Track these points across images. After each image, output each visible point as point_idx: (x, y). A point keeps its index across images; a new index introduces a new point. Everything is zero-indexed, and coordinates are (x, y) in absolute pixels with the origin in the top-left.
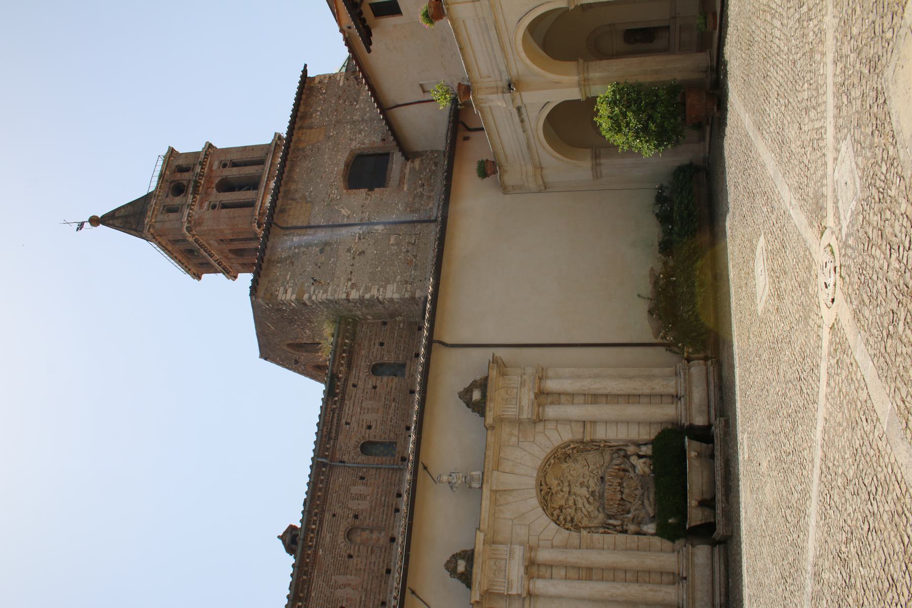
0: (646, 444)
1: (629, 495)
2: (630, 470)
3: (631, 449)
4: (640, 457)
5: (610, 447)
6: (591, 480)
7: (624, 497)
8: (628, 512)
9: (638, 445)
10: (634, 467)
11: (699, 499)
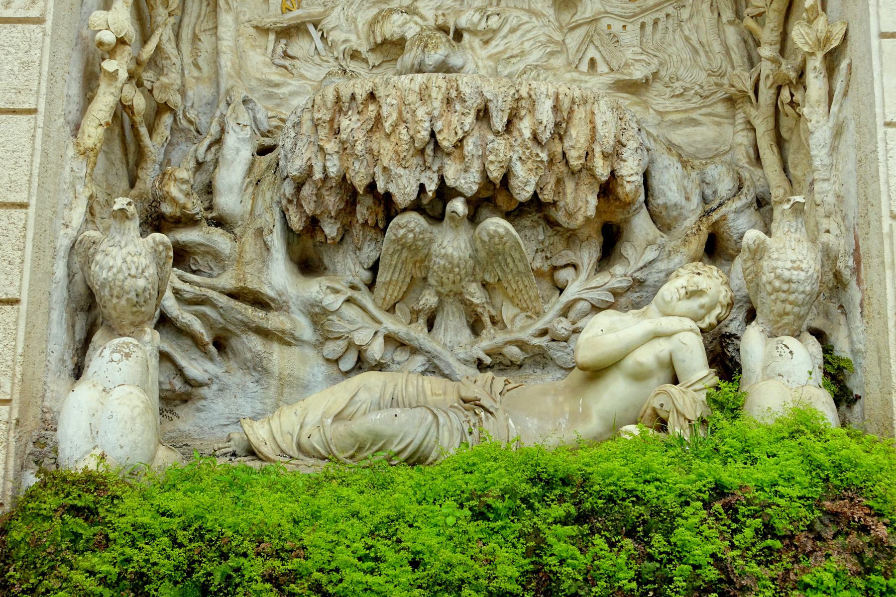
1: (418, 255)
2: (618, 275)
3: (789, 255)
8: (307, 266)
10: (636, 294)
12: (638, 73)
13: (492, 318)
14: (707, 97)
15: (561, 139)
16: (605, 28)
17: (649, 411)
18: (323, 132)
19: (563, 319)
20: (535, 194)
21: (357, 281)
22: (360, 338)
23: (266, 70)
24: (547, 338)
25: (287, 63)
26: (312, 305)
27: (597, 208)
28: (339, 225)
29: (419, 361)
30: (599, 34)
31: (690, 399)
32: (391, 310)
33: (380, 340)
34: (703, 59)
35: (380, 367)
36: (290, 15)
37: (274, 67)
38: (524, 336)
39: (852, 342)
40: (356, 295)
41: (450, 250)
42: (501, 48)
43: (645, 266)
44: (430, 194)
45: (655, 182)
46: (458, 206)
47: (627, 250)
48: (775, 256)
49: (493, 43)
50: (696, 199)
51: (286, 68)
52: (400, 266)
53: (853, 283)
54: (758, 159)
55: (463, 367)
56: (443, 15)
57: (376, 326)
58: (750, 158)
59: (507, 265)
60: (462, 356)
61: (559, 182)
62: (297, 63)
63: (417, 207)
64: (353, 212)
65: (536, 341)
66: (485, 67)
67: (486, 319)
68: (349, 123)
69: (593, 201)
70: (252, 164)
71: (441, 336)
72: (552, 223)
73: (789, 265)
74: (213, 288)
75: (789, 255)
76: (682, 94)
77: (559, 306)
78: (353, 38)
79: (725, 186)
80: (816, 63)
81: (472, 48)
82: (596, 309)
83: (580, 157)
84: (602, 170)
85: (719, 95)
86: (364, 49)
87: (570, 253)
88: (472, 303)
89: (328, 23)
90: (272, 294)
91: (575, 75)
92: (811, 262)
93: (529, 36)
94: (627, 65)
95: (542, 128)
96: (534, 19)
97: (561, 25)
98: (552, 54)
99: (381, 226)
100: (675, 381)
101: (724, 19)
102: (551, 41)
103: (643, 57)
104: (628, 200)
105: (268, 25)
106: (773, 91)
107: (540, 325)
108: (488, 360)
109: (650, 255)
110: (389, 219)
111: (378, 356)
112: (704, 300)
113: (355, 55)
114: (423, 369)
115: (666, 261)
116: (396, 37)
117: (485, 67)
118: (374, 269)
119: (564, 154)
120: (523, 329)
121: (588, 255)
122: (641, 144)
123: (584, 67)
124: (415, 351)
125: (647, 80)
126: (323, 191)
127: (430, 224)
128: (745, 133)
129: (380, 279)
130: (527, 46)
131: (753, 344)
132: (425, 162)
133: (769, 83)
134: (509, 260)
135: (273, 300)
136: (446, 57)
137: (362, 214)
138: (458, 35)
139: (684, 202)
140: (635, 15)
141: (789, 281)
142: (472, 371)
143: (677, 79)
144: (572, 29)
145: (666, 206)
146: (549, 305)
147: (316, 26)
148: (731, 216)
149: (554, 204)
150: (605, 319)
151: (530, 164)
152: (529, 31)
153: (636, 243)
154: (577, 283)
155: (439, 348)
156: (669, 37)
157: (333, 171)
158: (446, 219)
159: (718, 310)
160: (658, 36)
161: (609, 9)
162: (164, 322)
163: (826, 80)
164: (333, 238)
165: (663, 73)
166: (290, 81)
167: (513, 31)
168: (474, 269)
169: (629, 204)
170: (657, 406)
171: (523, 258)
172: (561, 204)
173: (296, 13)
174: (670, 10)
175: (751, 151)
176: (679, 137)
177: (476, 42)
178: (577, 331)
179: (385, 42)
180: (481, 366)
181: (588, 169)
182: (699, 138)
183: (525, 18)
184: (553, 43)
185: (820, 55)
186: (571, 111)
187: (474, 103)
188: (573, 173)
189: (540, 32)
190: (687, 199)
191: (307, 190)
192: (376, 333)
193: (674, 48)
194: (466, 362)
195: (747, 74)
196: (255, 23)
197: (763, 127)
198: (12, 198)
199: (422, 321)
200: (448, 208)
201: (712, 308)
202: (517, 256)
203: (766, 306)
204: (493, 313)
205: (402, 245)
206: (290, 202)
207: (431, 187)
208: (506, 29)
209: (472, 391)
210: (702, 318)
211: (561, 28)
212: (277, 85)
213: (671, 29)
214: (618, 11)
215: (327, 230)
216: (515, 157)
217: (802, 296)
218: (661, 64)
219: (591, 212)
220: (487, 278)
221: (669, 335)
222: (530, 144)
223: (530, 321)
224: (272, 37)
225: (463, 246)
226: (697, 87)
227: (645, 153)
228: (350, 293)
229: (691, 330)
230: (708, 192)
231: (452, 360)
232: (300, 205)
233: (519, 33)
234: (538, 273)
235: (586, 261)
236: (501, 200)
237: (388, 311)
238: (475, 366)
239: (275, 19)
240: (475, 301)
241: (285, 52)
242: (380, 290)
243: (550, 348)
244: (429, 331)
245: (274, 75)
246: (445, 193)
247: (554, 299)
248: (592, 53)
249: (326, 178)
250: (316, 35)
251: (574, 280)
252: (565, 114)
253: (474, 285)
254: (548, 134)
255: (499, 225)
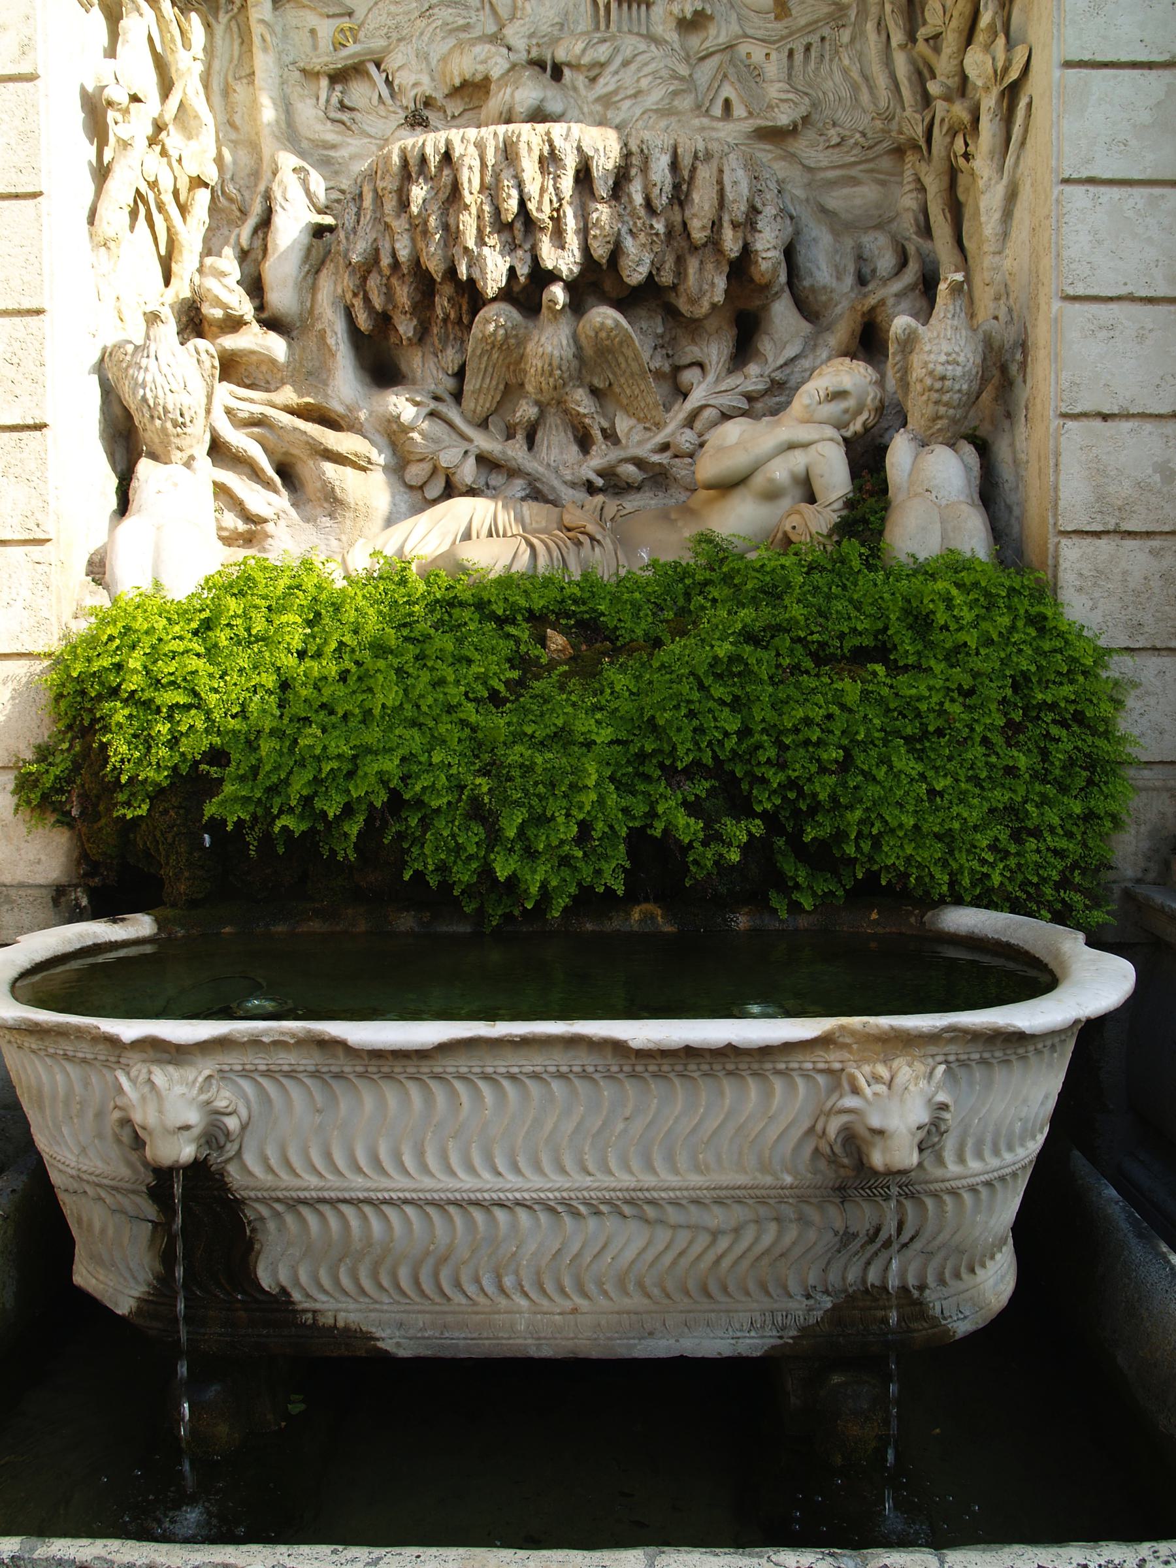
0: (989, 492)
2: (753, 377)
4: (867, 457)
5: (956, 210)
6: (656, 59)
7: (495, 320)
9: (988, 410)
10: (772, 398)
11: (252, 1171)
12: (783, 118)
13: (603, 430)
14: (870, 148)
15: (681, 204)
16: (744, 57)
17: (780, 535)
18: (390, 204)
19: (687, 431)
20: (650, 275)
21: (440, 391)
22: (448, 458)
23: (319, 127)
24: (668, 454)
25: (345, 117)
26: (389, 421)
27: (726, 291)
28: (415, 322)
29: (518, 487)
30: (735, 66)
31: (820, 520)
32: (483, 425)
33: (471, 461)
34: (865, 97)
35: (472, 492)
36: (344, 53)
37: (329, 123)
38: (641, 452)
39: (1014, 452)
40: (442, 408)
41: (549, 349)
42: (611, 88)
43: (785, 364)
44: (522, 279)
45: (801, 260)
46: (558, 292)
47: (766, 346)
48: (927, 348)
49: (602, 81)
50: (849, 280)
51: (343, 123)
52: (490, 370)
53: (1020, 379)
54: (926, 230)
55: (571, 491)
56: (538, 45)
57: (465, 446)
58: (918, 226)
59: (619, 365)
60: (569, 478)
61: (680, 261)
62: (357, 116)
63: (506, 294)
64: (431, 306)
65: (656, 458)
66: (591, 113)
67: (597, 433)
68: (418, 192)
69: (721, 283)
70: (309, 250)
71: (544, 454)
72: (672, 313)
73: (943, 358)
74: (274, 406)
75: (941, 347)
76: (838, 145)
77: (682, 416)
78: (425, 79)
79: (886, 262)
80: (989, 103)
81: (575, 89)
82: (726, 417)
83: (704, 228)
84: (731, 243)
85: (885, 145)
86: (439, 96)
87: (696, 349)
88: (578, 414)
89: (393, 62)
90: (340, 409)
91: (705, 121)
92: (970, 355)
93: (647, 70)
94: (770, 107)
95: (656, 191)
96: (653, 47)
97: (688, 56)
98: (675, 93)
99: (465, 321)
100: (811, 499)
101: (894, 43)
102: (675, 76)
103: (791, 96)
104: (763, 281)
105: (318, 68)
106: (948, 139)
107: (660, 438)
108: (600, 482)
109: (790, 352)
110: (474, 312)
111: (469, 480)
112: (850, 403)
113: (428, 103)
114: (523, 494)
115: (811, 357)
116: (479, 77)
117: (591, 113)
118: (460, 375)
119: (685, 224)
120: (640, 443)
121: (716, 351)
122: (781, 210)
123: (717, 111)
124: (513, 472)
125: (795, 126)
126: (394, 281)
127: (524, 317)
128: (914, 195)
129: (467, 388)
130: (644, 83)
131: (900, 454)
132: (514, 238)
133: (945, 130)
134: (621, 359)
135: (342, 417)
136: (542, 101)
137: (443, 307)
138: (557, 73)
139: (834, 284)
140: (783, 38)
141: (943, 378)
142: (581, 495)
143: (834, 125)
144: (703, 59)
145: (812, 289)
146: (671, 414)
147: (378, 66)
148: (891, 301)
149: (674, 287)
150: (733, 430)
151: (642, 237)
152: (646, 64)
153: (776, 336)
154: (703, 386)
155: (541, 469)
156: (825, 68)
157: (404, 254)
158: (544, 310)
159: (865, 416)
160: (812, 65)
161: (750, 32)
162: (218, 449)
163: (1003, 124)
164: (409, 339)
165: (815, 117)
166: (349, 140)
167: (626, 64)
168: (580, 371)
169: (767, 286)
170: (788, 528)
171: (637, 357)
172: (681, 288)
173: (352, 48)
174: (826, 32)
175: (921, 218)
176: (835, 200)
177: (580, 80)
178: (702, 445)
179: (465, 84)
180: (591, 488)
181: (714, 242)
182: (858, 202)
183: (642, 46)
184: (676, 78)
185: (995, 91)
186: (693, 169)
187: (571, 162)
188: (696, 249)
189: (662, 65)
190: (839, 279)
191: (373, 282)
192: (466, 452)
193: (830, 83)
194: (573, 485)
195: (918, 116)
196: (302, 65)
197: (934, 186)
198: (26, 305)
199: (520, 436)
200: (545, 297)
201: (859, 412)
202: (629, 353)
203: (918, 409)
204: (606, 425)
205: (492, 344)
206: (355, 295)
207: (523, 271)
208: (618, 61)
209: (573, 517)
210: (846, 426)
211: (687, 59)
212: (334, 147)
213: (827, 57)
214: (760, 34)
215: (401, 329)
216: (624, 230)
217: (957, 396)
218: (814, 105)
219: (719, 297)
220: (597, 382)
221: (805, 446)
222: (642, 212)
223: (648, 434)
224: (324, 83)
225: (565, 342)
226: (858, 135)
227: (788, 221)
228: (433, 405)
229: (831, 440)
230: (866, 270)
231: (556, 483)
232: (367, 300)
233: (633, 67)
234: (658, 375)
235: (714, 358)
236: (608, 285)
237: (479, 426)
238: (584, 489)
239: (326, 59)
240: (582, 410)
241: (341, 102)
242: (468, 402)
243: (672, 466)
244: (530, 448)
245: (329, 133)
246: (542, 277)
247: (676, 407)
248: (728, 91)
249: (396, 265)
250: (379, 78)
251: (700, 383)
252: (686, 174)
253: (580, 391)
254: (664, 200)
255: (607, 317)
